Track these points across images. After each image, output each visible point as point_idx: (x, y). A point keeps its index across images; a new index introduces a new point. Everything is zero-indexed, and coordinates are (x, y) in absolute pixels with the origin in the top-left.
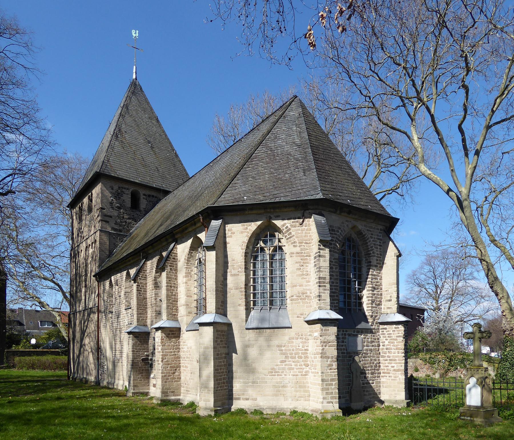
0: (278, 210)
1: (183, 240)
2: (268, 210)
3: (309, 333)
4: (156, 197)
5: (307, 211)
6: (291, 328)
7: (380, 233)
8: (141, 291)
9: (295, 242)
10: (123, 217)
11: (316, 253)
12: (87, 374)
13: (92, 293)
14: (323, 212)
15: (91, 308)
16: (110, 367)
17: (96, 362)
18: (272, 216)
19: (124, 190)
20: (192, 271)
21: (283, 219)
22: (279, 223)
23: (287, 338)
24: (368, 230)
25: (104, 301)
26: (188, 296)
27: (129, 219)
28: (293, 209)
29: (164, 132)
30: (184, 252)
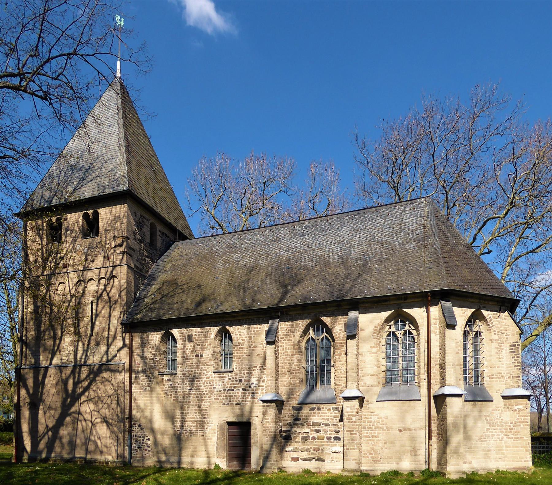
0: (486, 302)
1: (370, 310)
2: (481, 301)
3: (503, 406)
6: (492, 401)
9: (495, 331)
10: (144, 254)
11: (514, 342)
12: (87, 452)
13: (98, 344)
15: (101, 366)
16: (166, 441)
17: (120, 436)
21: (488, 310)
22: (485, 313)
23: (490, 409)
25: (143, 357)
26: (377, 367)
27: (148, 257)
28: (496, 303)
30: (371, 322)
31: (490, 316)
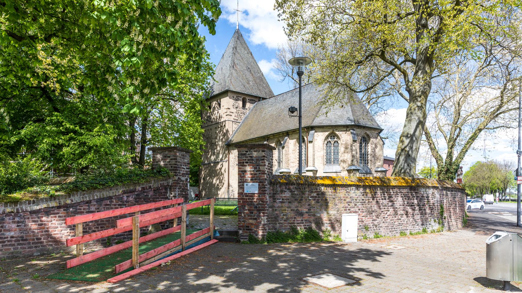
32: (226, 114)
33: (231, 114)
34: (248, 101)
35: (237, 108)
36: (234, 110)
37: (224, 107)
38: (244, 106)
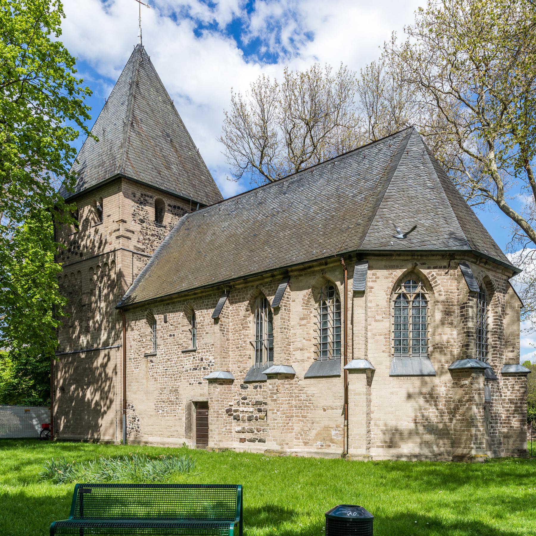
0: (425, 258)
2: (416, 257)
4: (182, 209)
5: (453, 261)
7: (504, 283)
8: (224, 331)
9: (440, 291)
14: (467, 263)
18: (418, 263)
19: (147, 198)
20: (311, 312)
21: (429, 268)
24: (496, 281)
27: (153, 235)
28: (440, 257)
29: (181, 122)
31: (433, 273)
32: (117, 234)
33: (129, 234)
34: (167, 208)
35: (142, 221)
36: (137, 227)
37: (111, 219)
38: (159, 219)
